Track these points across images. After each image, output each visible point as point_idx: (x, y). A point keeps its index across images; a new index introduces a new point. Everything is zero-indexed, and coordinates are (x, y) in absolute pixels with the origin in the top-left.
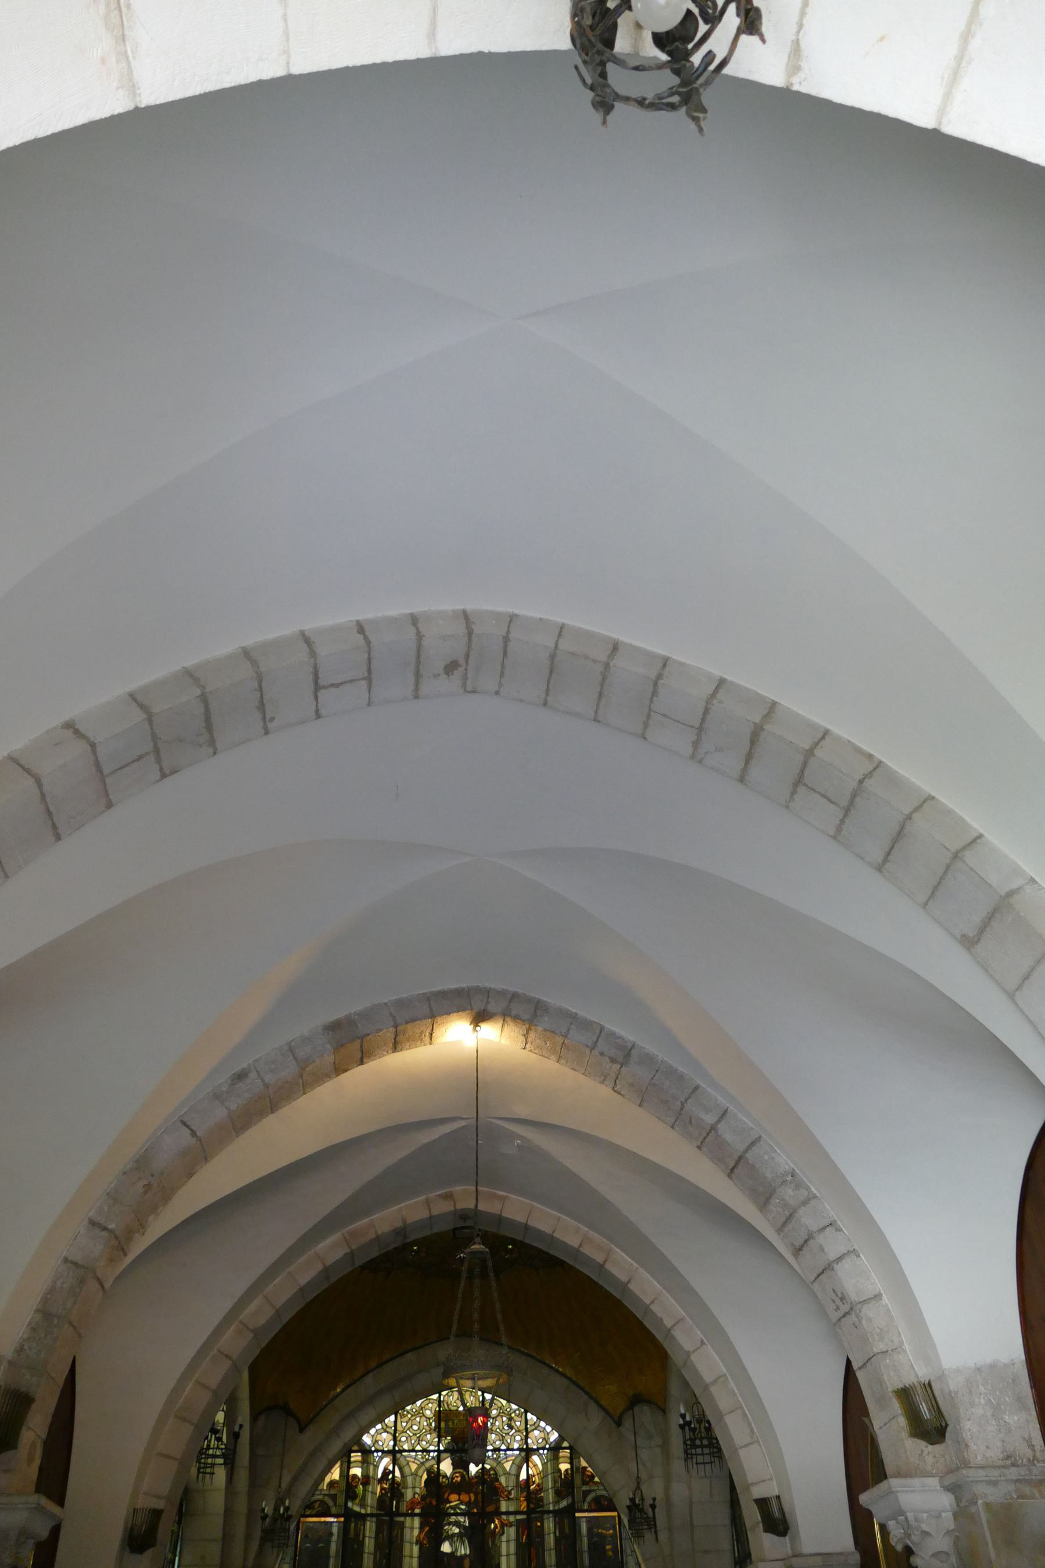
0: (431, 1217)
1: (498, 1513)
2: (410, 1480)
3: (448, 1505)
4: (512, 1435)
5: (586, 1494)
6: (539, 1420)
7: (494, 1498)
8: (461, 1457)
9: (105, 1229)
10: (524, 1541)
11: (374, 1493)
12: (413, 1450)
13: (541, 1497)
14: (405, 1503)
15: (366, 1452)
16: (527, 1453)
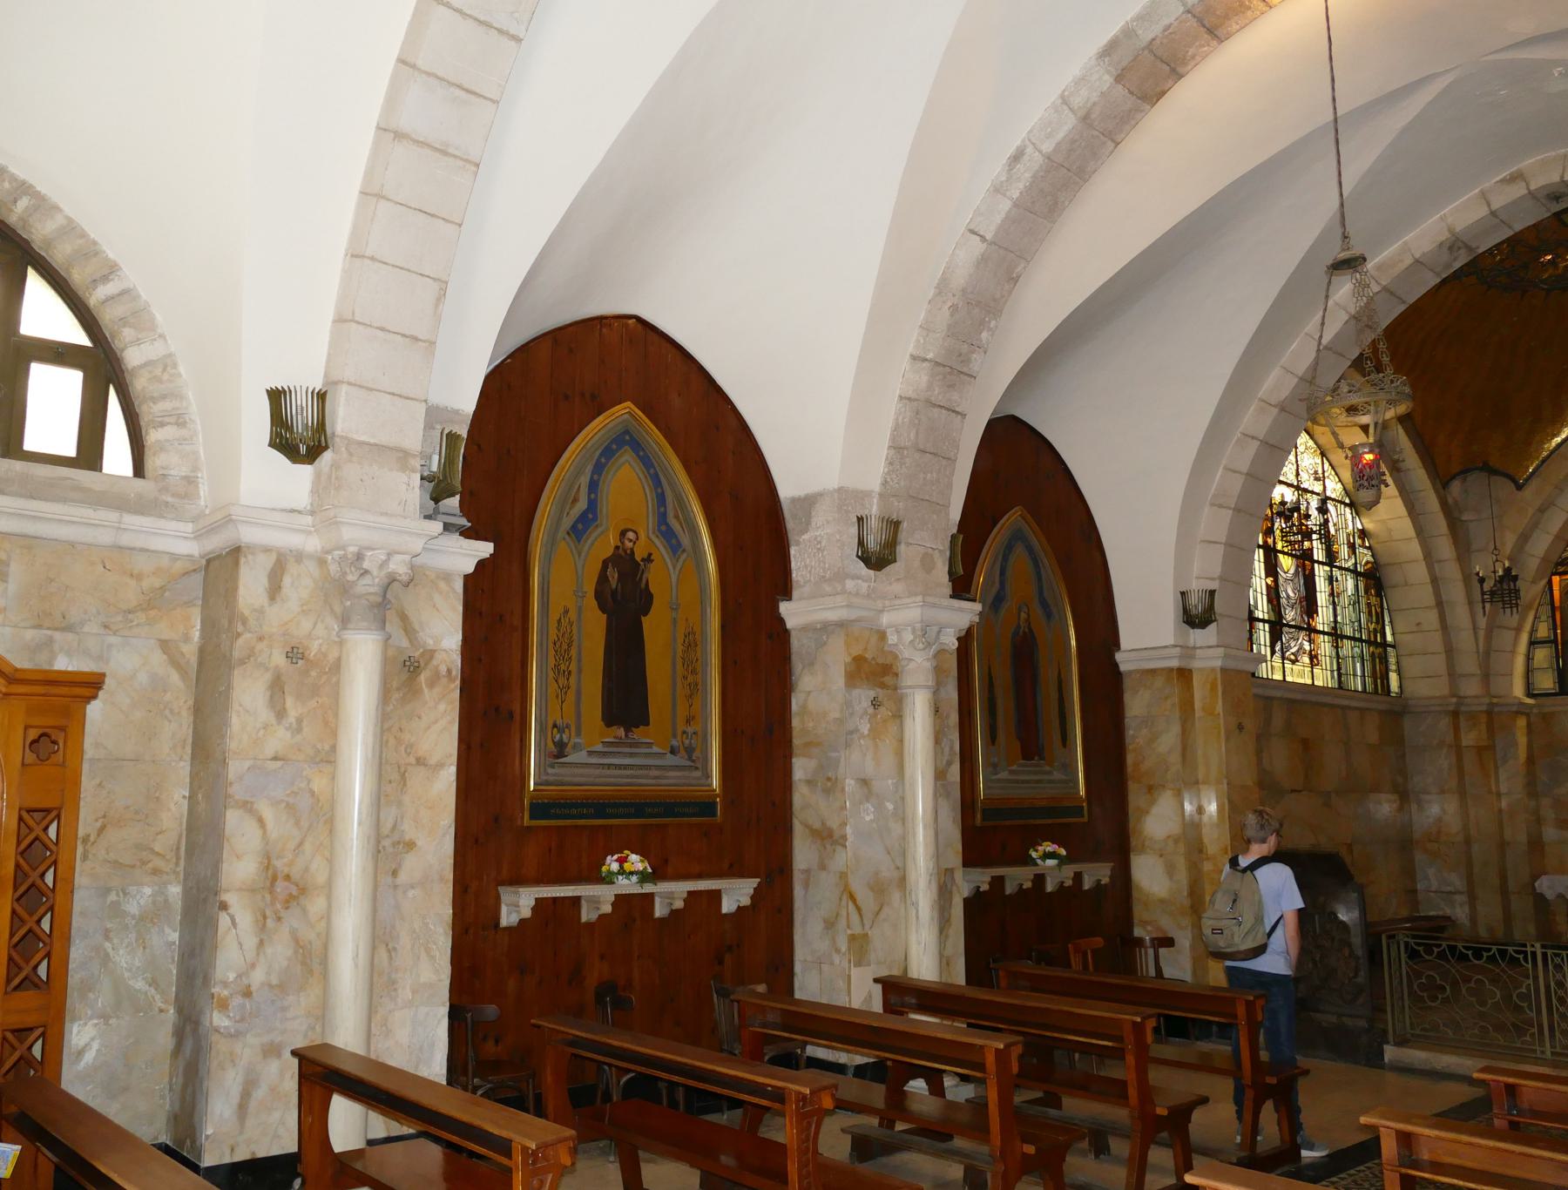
0: (1493, 214)
9: (926, 360)
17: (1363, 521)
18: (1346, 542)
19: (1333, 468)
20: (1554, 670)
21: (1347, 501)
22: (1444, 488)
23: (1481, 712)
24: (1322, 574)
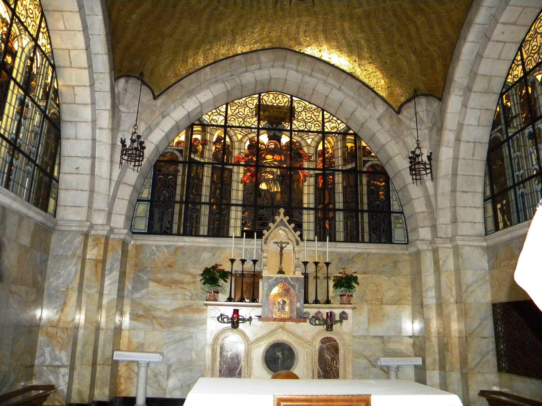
2: (237, 144)
3: (265, 161)
4: (313, 123)
5: (365, 162)
6: (332, 116)
8: (275, 133)
10: (320, 186)
11: (210, 150)
12: (240, 127)
13: (333, 161)
15: (204, 126)
17: (59, 83)
18: (43, 87)
19: (48, 30)
20: (147, 218)
21: (52, 61)
22: (115, 80)
23: (103, 236)
24: (16, 92)
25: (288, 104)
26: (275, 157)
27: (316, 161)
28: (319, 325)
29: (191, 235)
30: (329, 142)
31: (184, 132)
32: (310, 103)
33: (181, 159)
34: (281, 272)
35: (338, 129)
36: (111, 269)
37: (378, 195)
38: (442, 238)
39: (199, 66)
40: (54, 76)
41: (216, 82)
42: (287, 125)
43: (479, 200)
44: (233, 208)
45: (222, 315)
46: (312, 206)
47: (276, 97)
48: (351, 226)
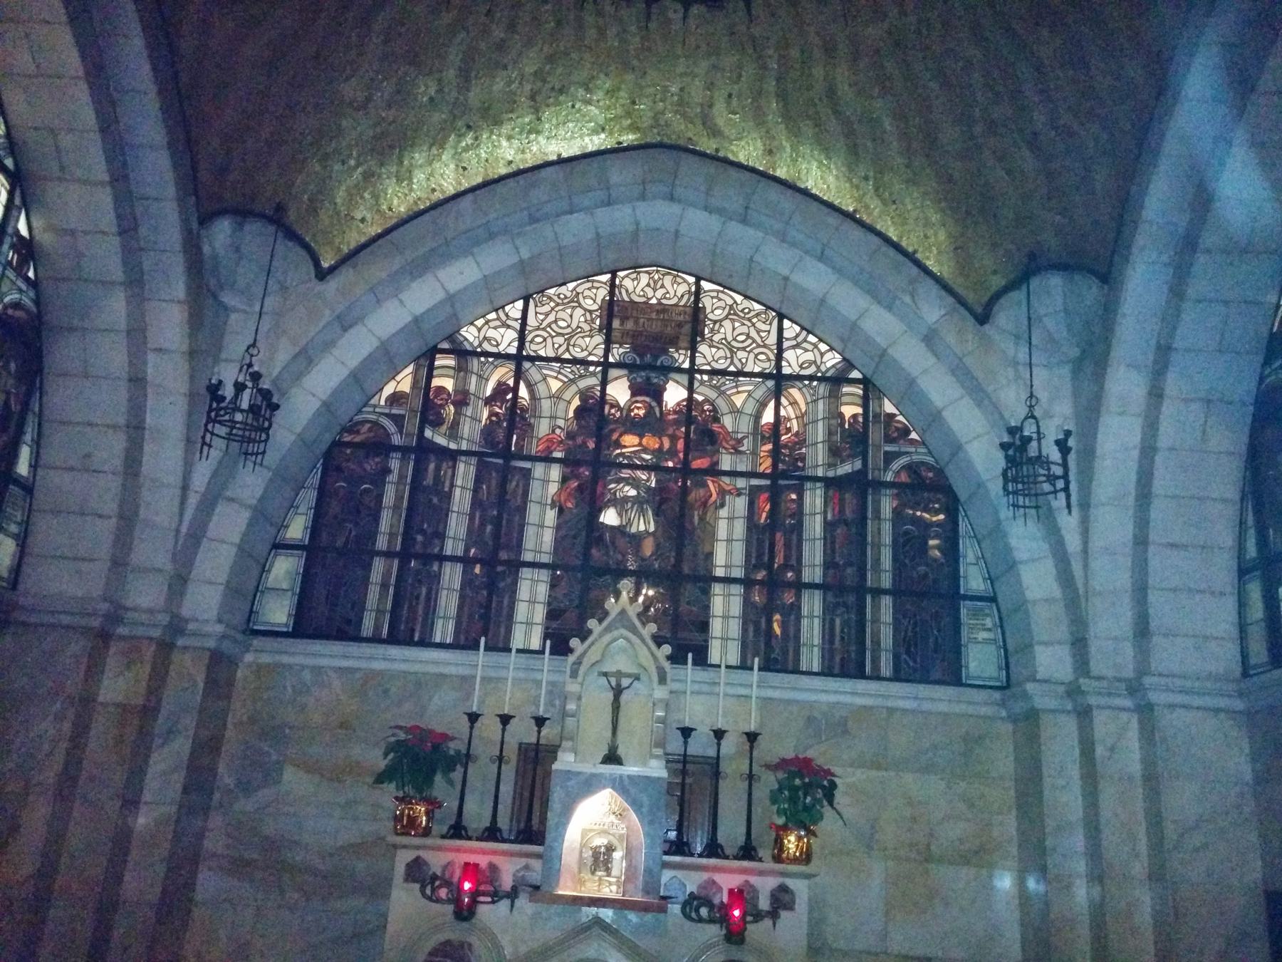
1: (714, 471)
2: (546, 405)
3: (618, 451)
4: (751, 351)
5: (889, 458)
6: (804, 333)
7: (709, 448)
8: (648, 379)
10: (762, 521)
11: (475, 419)
14: (535, 441)
15: (463, 354)
16: (779, 381)
17: (35, 224)
23: (151, 639)
25: (689, 299)
26: (644, 441)
27: (754, 453)
28: (711, 921)
29: (409, 642)
30: (794, 403)
31: (410, 369)
32: (746, 297)
33: (397, 440)
34: (612, 758)
35: (818, 367)
36: (170, 732)
37: (924, 548)
38: (1099, 678)
39: (443, 192)
40: (17, 201)
41: (492, 236)
42: (682, 358)
43: (1222, 569)
44: (526, 573)
45: (434, 877)
46: (738, 573)
47: (655, 282)
48: (842, 631)
